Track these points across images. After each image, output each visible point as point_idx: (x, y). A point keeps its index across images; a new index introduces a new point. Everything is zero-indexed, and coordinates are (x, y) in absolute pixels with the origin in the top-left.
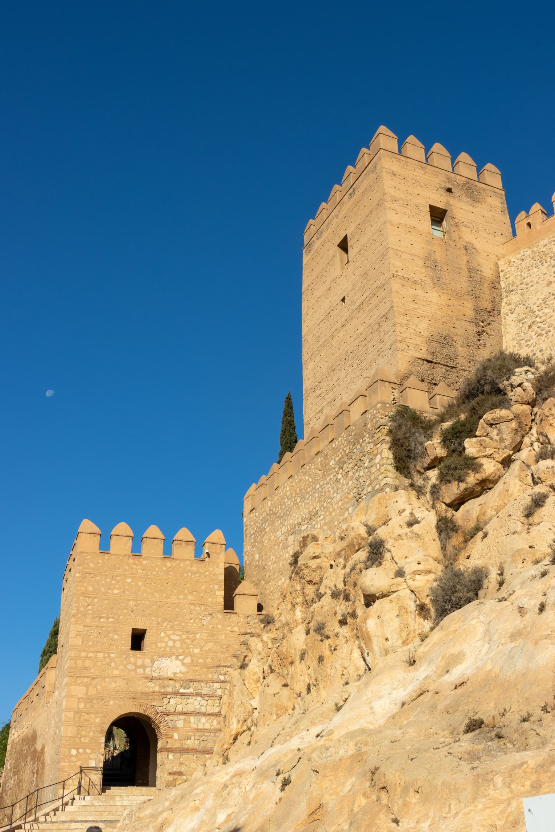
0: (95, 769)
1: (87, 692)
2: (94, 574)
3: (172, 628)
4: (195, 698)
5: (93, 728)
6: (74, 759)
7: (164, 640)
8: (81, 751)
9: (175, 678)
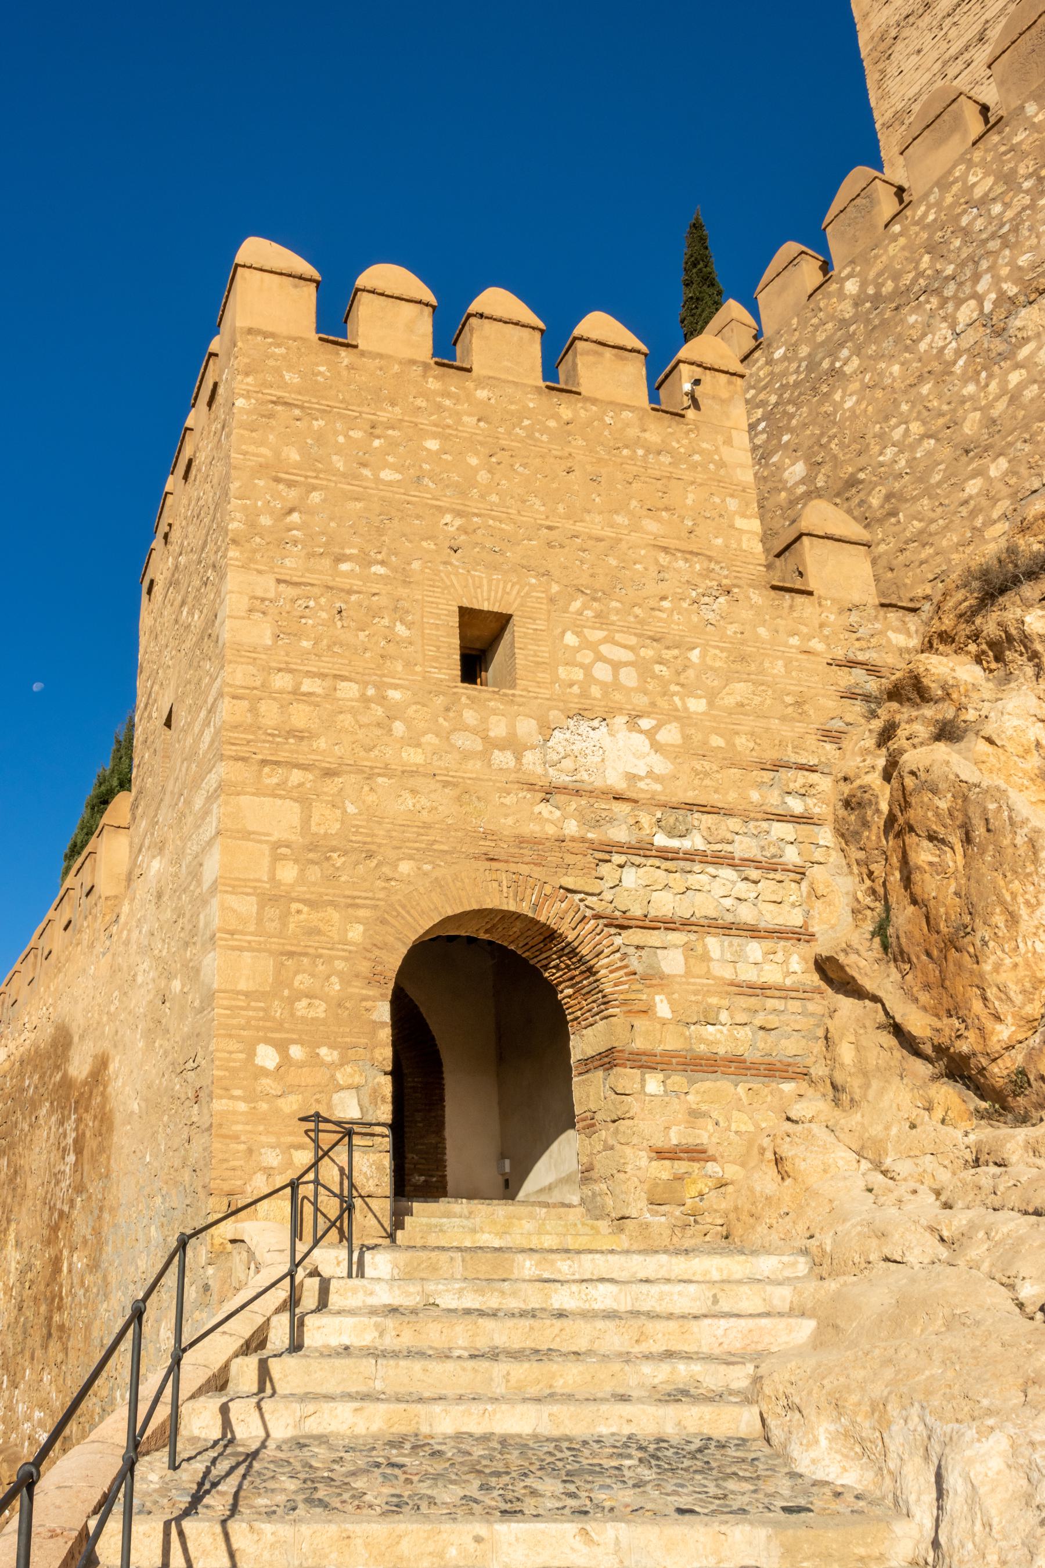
1: (306, 821)
2: (302, 407)
3: (601, 619)
4: (711, 870)
5: (340, 965)
7: (579, 658)
9: (634, 796)
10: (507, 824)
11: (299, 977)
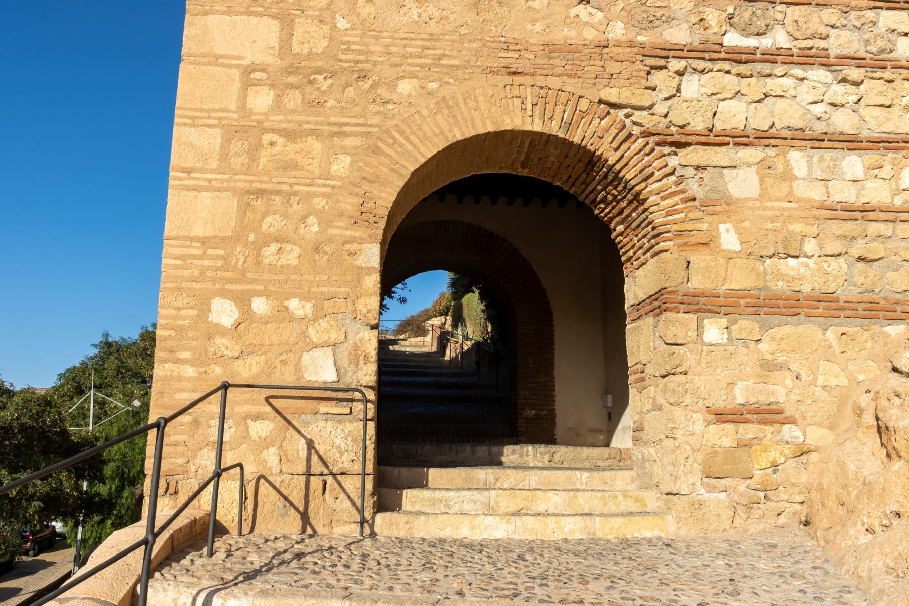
0: (337, 394)
4: (798, 71)
6: (222, 344)
8: (260, 306)
10: (535, 32)
11: (269, 219)
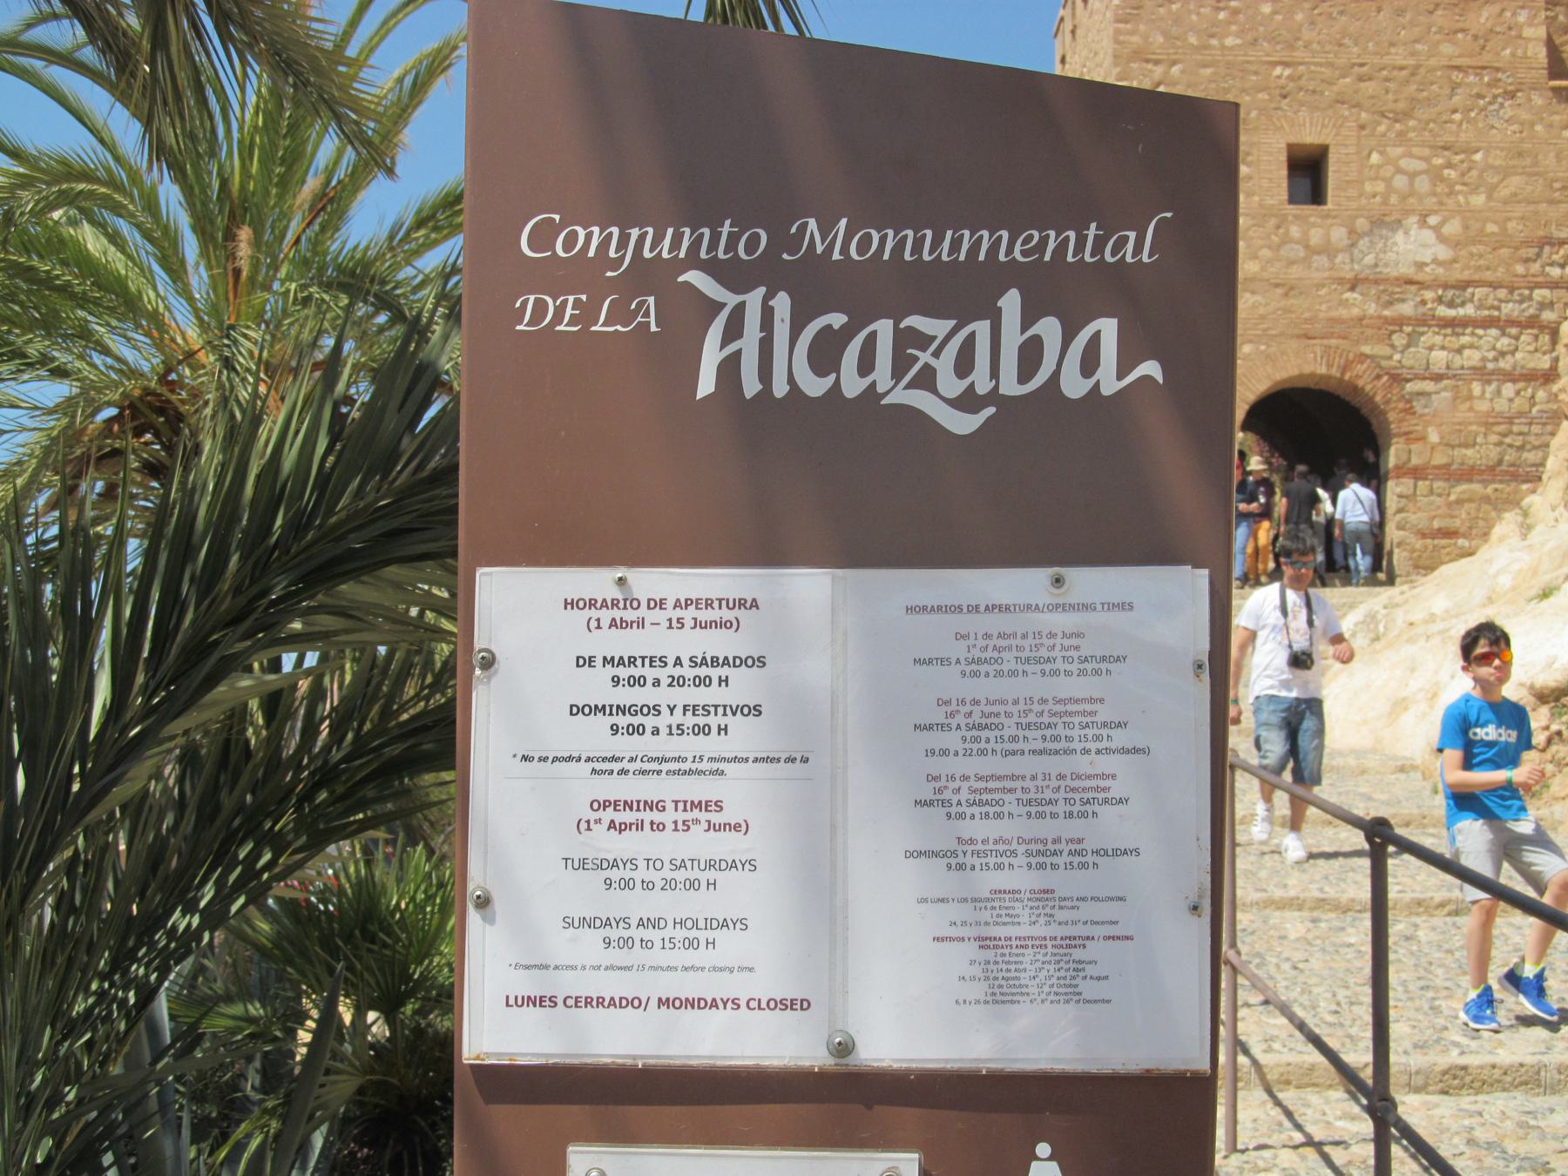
4: (1480, 332)
7: (1382, 173)
